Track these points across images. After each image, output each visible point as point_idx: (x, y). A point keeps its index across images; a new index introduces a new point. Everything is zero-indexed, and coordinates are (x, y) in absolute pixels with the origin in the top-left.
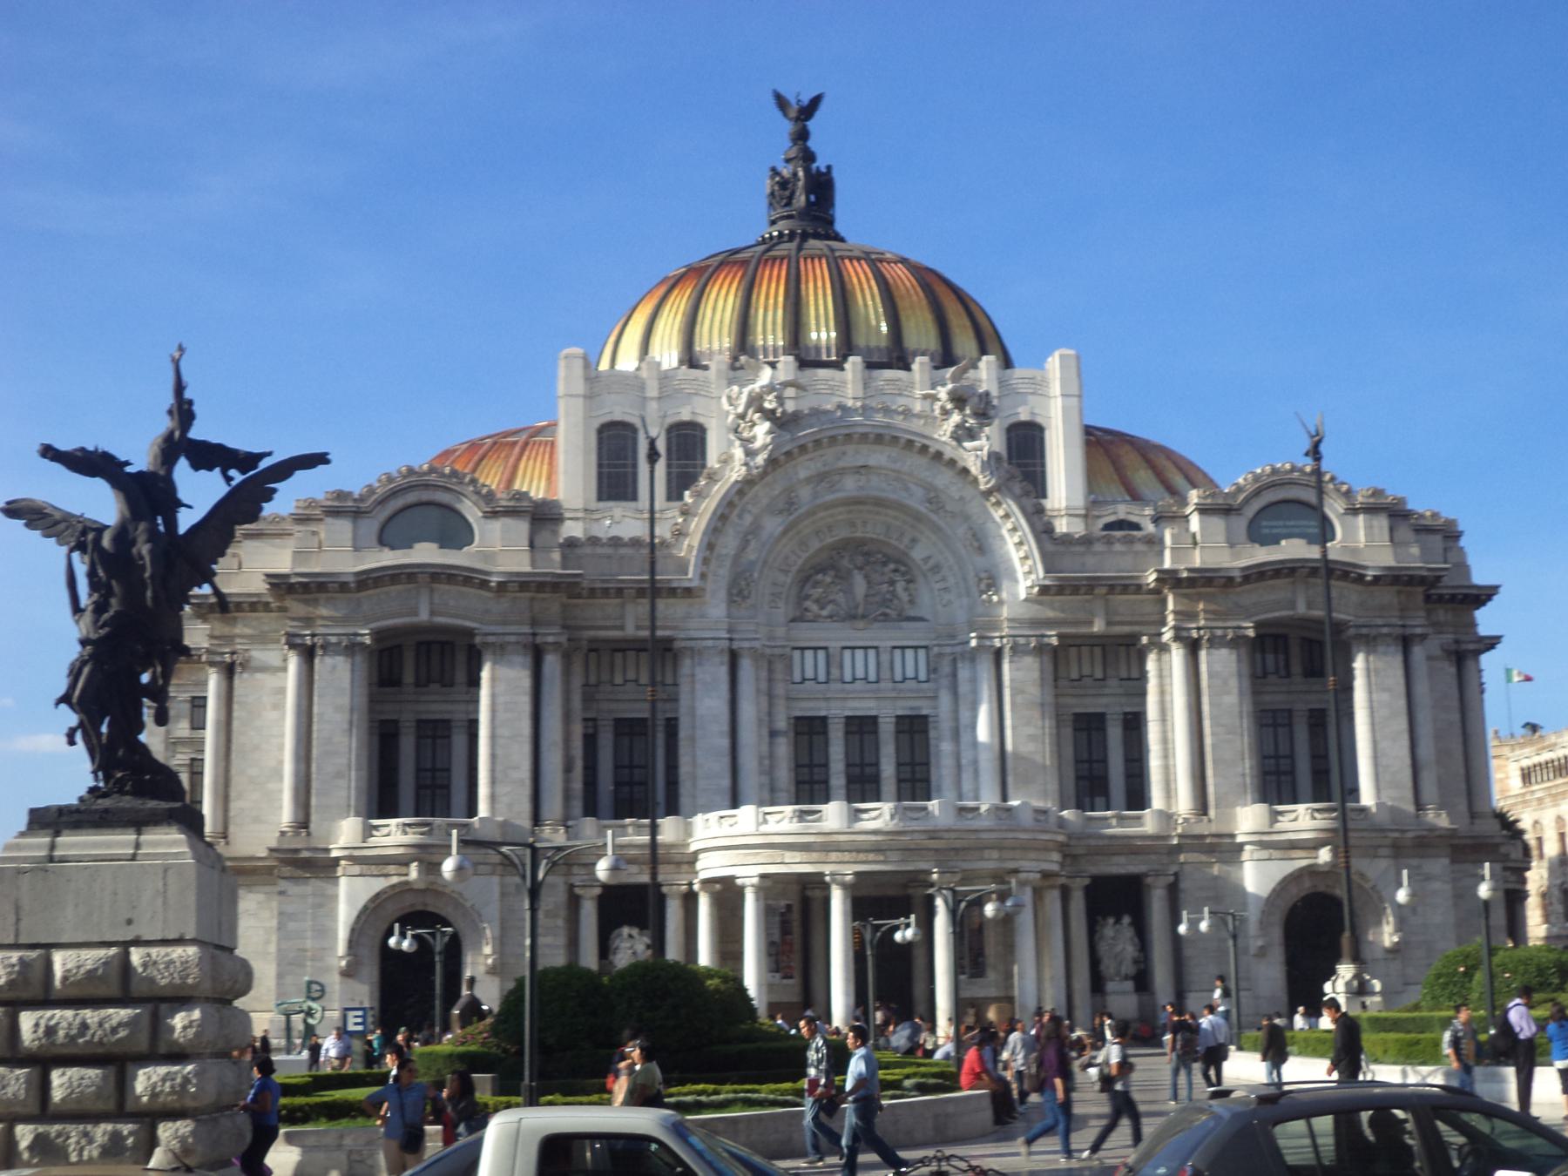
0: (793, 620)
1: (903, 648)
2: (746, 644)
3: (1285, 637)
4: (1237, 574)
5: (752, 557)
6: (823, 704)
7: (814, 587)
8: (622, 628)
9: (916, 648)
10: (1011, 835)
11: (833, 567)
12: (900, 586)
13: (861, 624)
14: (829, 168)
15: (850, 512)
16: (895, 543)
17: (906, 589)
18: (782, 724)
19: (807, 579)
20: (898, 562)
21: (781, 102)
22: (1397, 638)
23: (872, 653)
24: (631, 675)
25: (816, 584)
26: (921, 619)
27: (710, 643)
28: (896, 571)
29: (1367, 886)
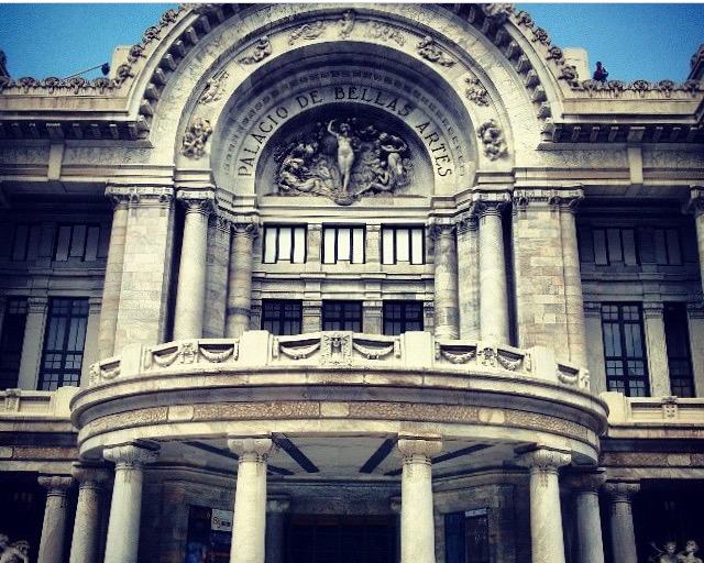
0: (268, 195)
1: (395, 228)
2: (195, 195)
6: (298, 288)
7: (295, 157)
9: (410, 228)
10: (521, 389)
11: (319, 141)
12: (392, 158)
15: (335, 74)
16: (389, 110)
18: (240, 299)
19: (287, 153)
20: (390, 134)
23: (358, 235)
24: (77, 251)
25: (298, 155)
26: (417, 196)
28: (387, 142)
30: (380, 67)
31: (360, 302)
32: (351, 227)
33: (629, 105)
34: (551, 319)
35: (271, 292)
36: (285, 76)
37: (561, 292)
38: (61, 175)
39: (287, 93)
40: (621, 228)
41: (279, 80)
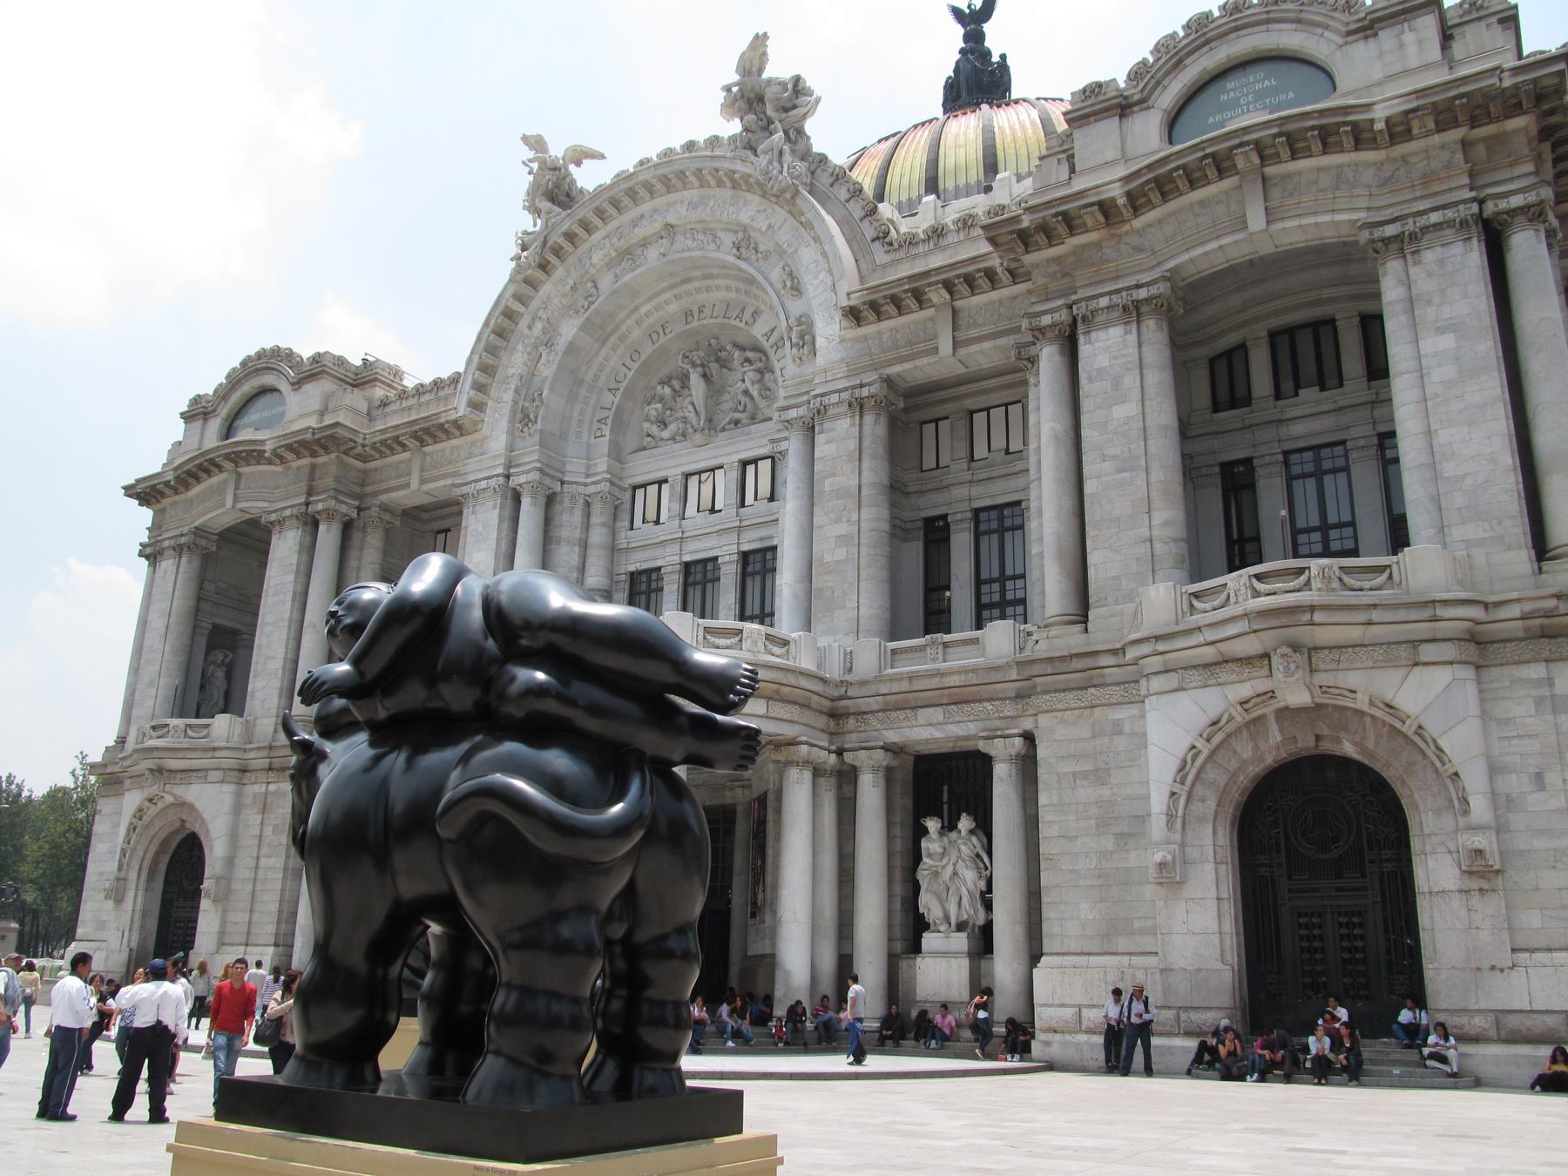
1: (755, 461)
3: (1331, 322)
4: (1116, 192)
5: (546, 373)
6: (659, 552)
8: (408, 485)
13: (698, 438)
14: (1003, 57)
16: (736, 323)
17: (760, 381)
20: (743, 349)
21: (957, 13)
22: (1464, 224)
27: (483, 484)
28: (748, 360)
29: (1408, 728)
30: (718, 276)
31: (716, 558)
32: (713, 470)
33: (948, 253)
34: (841, 554)
35: (636, 563)
36: (628, 316)
37: (855, 517)
38: (422, 482)
39: (636, 333)
40: (1006, 405)
41: (623, 321)
